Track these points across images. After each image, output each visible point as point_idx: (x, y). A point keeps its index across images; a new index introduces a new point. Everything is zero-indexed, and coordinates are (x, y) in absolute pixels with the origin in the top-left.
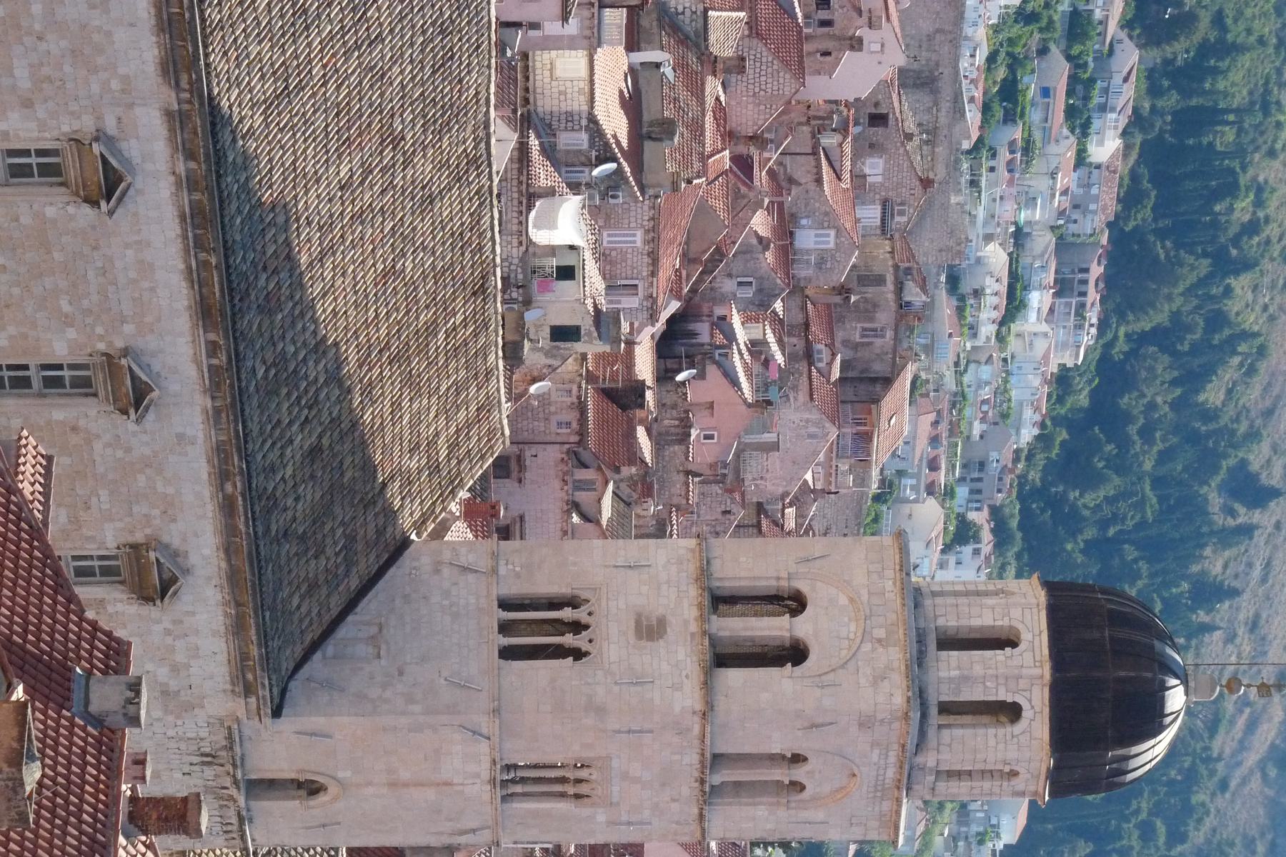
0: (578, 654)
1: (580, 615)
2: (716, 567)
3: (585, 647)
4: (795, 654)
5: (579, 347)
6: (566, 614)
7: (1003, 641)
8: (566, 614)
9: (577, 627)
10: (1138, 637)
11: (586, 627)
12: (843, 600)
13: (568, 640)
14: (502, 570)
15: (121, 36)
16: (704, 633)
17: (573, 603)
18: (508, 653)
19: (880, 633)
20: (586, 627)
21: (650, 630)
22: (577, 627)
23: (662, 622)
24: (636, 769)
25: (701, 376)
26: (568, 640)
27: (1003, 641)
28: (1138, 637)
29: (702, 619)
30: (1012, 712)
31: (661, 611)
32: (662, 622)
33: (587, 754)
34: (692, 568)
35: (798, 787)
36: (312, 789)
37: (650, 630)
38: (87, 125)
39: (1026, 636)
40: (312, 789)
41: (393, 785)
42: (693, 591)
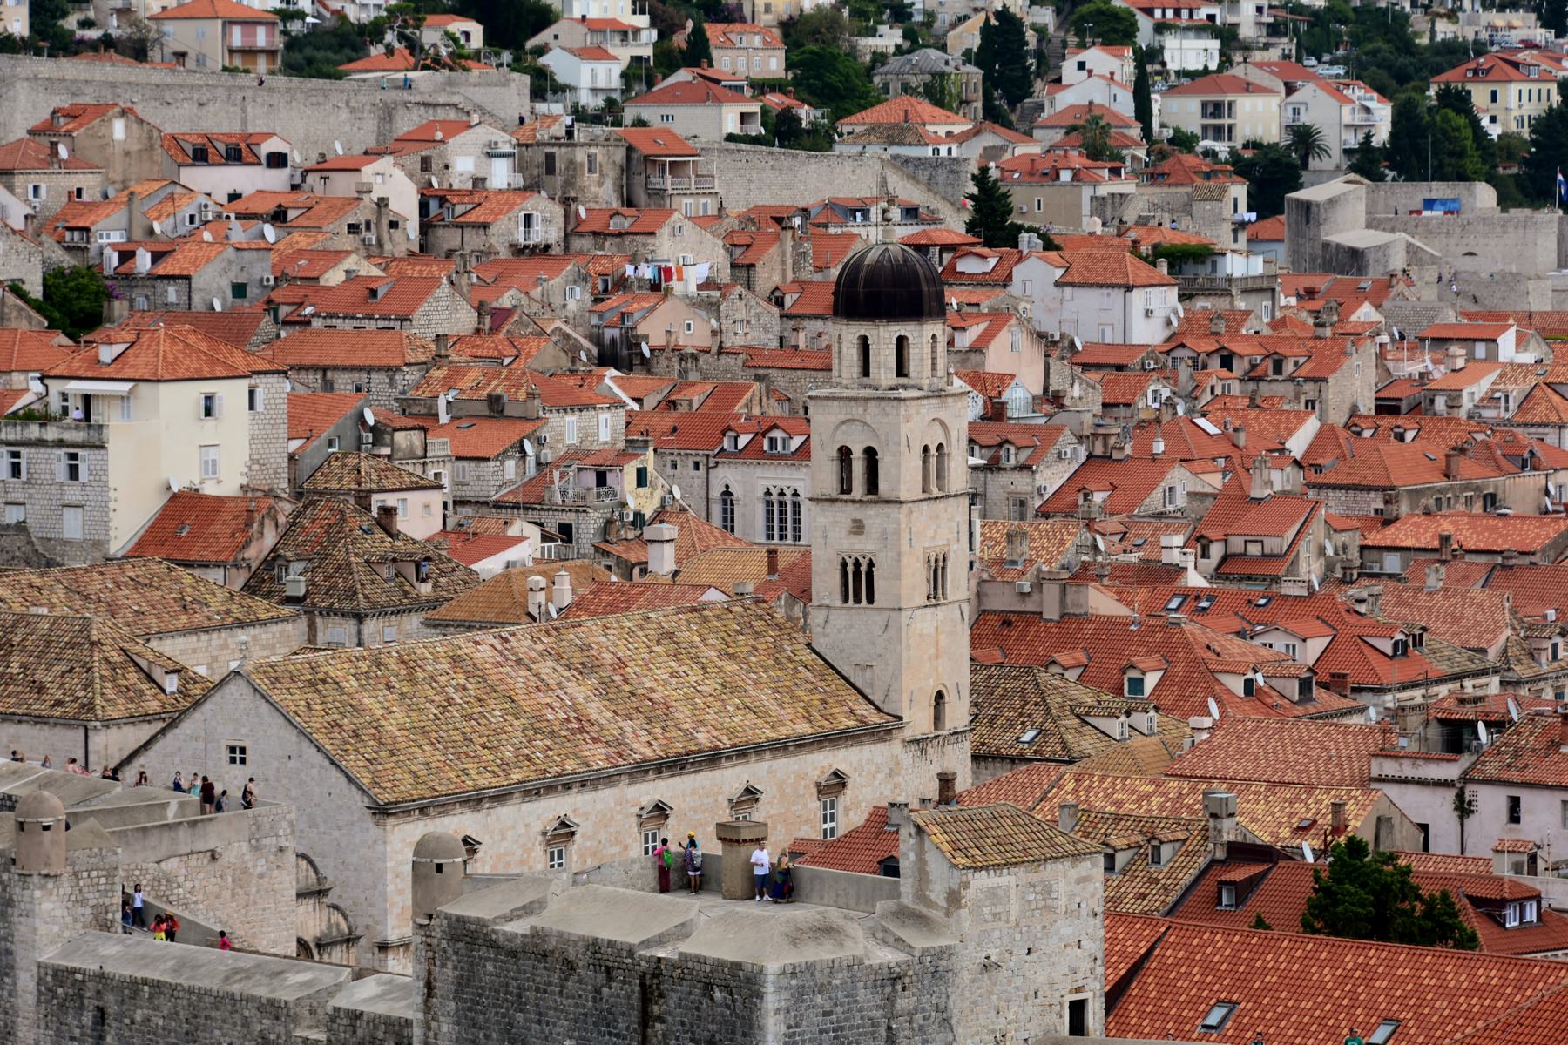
0: (871, 565)
1: (850, 562)
5: (650, 468)
6: (850, 569)
8: (850, 569)
9: (857, 564)
10: (862, 275)
13: (863, 569)
14: (827, 602)
15: (599, 806)
17: (844, 565)
18: (871, 600)
19: (861, 410)
21: (858, 527)
22: (857, 564)
24: (930, 533)
25: (646, 337)
26: (863, 569)
27: (864, 342)
28: (862, 275)
29: (854, 501)
30: (901, 342)
31: (849, 522)
33: (922, 559)
34: (827, 505)
35: (940, 447)
36: (940, 696)
37: (858, 527)
38: (634, 820)
39: (863, 332)
40: (940, 696)
41: (937, 657)
42: (839, 505)
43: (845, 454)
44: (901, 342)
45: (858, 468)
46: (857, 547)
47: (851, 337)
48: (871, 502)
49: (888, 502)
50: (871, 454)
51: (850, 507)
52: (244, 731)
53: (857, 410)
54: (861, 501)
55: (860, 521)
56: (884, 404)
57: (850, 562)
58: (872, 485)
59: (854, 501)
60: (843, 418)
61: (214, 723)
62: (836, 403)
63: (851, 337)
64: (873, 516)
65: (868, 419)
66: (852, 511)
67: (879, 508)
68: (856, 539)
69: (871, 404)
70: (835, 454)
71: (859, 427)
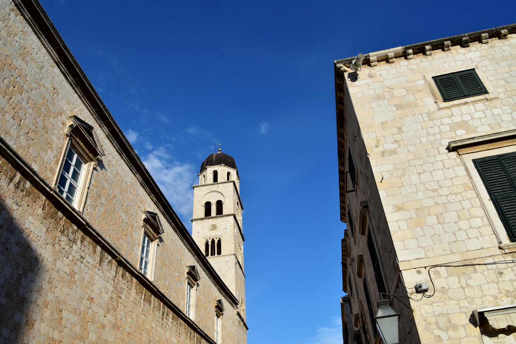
2: (199, 217)
3: (218, 239)
6: (210, 243)
7: (215, 174)
8: (210, 243)
9: (213, 241)
11: (213, 239)
12: (208, 195)
13: (216, 242)
16: (216, 217)
18: (219, 253)
19: (216, 188)
20: (213, 239)
22: (213, 241)
26: (216, 242)
27: (215, 174)
29: (213, 218)
31: (210, 226)
32: (212, 225)
34: (200, 221)
37: (214, 227)
39: (215, 169)
42: (205, 221)
43: (208, 205)
44: (229, 174)
49: (228, 215)
51: (211, 220)
54: (216, 217)
55: (215, 225)
58: (220, 212)
60: (208, 191)
64: (220, 222)
65: (219, 190)
67: (224, 218)
70: (204, 204)
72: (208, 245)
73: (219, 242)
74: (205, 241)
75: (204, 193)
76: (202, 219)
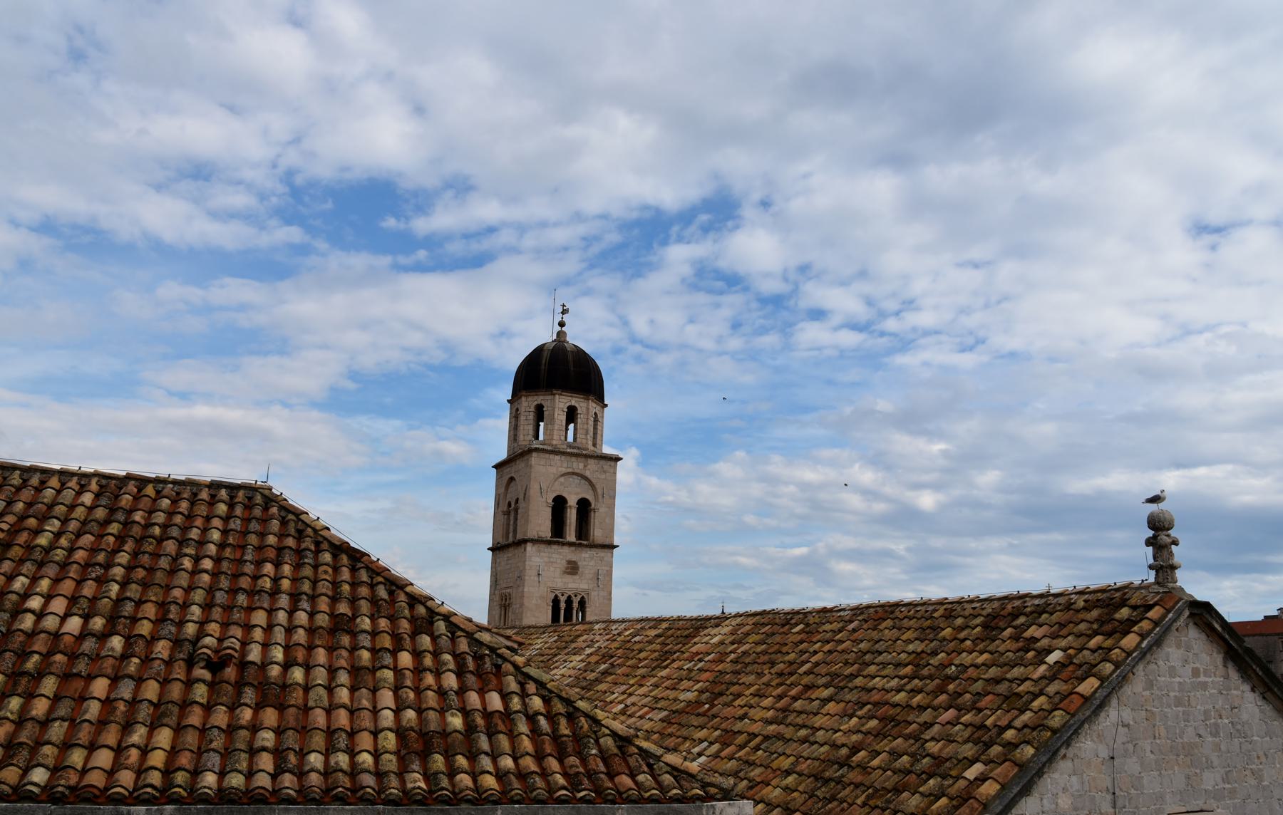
1: (563, 599)
3: (579, 598)
4: (584, 506)
6: (563, 605)
8: (563, 605)
9: (569, 601)
10: (570, 358)
11: (569, 597)
12: (562, 479)
19: (581, 465)
21: (572, 568)
22: (569, 601)
23: (569, 562)
29: (571, 544)
32: (569, 562)
34: (542, 547)
37: (572, 568)
39: (573, 403)
42: (555, 547)
43: (559, 505)
45: (572, 516)
46: (571, 585)
47: (561, 405)
48: (586, 546)
50: (584, 506)
51: (566, 550)
52: (1210, 780)
53: (578, 466)
55: (575, 563)
56: (602, 462)
57: (563, 599)
59: (571, 544)
60: (564, 470)
61: (1132, 766)
62: (557, 457)
63: (561, 405)
64: (586, 558)
65: (588, 474)
66: (566, 553)
67: (593, 552)
68: (569, 578)
69: (591, 461)
71: (576, 480)
72: (559, 610)
73: (582, 603)
74: (552, 596)
75: (553, 470)
76: (549, 543)
